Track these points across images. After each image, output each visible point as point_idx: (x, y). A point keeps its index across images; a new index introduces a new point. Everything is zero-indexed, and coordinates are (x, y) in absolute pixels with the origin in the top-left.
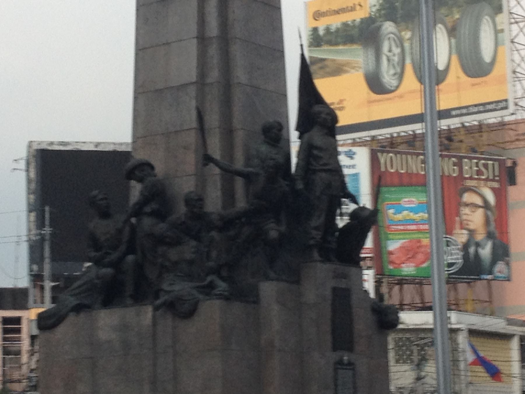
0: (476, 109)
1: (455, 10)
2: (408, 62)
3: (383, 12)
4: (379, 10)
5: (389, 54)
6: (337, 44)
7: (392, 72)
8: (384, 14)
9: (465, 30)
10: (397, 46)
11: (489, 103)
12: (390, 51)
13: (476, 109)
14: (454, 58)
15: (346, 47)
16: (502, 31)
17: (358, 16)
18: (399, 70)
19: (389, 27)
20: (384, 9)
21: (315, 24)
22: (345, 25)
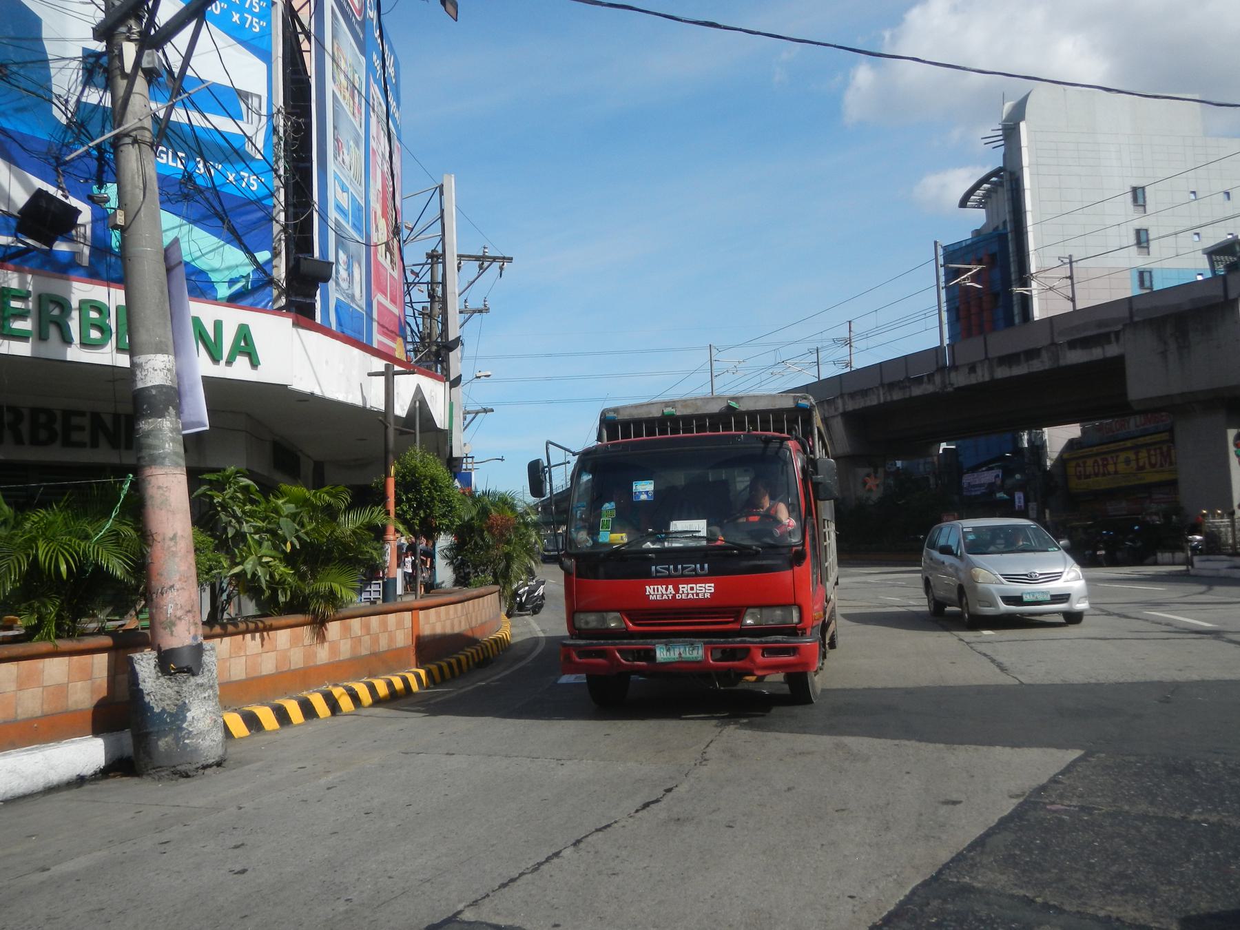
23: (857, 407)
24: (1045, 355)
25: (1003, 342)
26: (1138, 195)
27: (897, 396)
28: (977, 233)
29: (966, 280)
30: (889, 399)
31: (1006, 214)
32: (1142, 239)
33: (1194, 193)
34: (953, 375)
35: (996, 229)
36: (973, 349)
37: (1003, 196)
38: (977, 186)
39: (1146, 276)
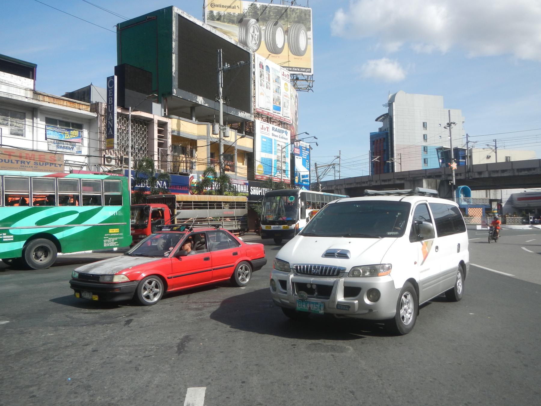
0: (296, 69)
1: (288, 23)
2: (263, 39)
3: (251, 14)
4: (249, 13)
5: (253, 34)
6: (224, 22)
7: (254, 42)
8: (251, 15)
9: (292, 33)
10: (258, 32)
11: (303, 68)
12: (254, 32)
13: (296, 69)
14: (286, 44)
15: (228, 24)
16: (310, 39)
17: (237, 12)
18: (257, 42)
19: (253, 21)
20: (252, 13)
21: (212, 9)
22: (229, 14)
23: (349, 187)
24: (392, 181)
25: (384, 176)
26: (425, 125)
27: (359, 186)
28: (380, 129)
29: (375, 159)
30: (357, 186)
31: (388, 126)
32: (425, 137)
33: (440, 124)
34: (372, 182)
35: (385, 130)
36: (377, 177)
37: (388, 120)
38: (381, 117)
39: (426, 148)
